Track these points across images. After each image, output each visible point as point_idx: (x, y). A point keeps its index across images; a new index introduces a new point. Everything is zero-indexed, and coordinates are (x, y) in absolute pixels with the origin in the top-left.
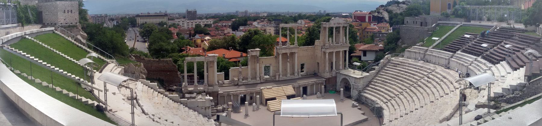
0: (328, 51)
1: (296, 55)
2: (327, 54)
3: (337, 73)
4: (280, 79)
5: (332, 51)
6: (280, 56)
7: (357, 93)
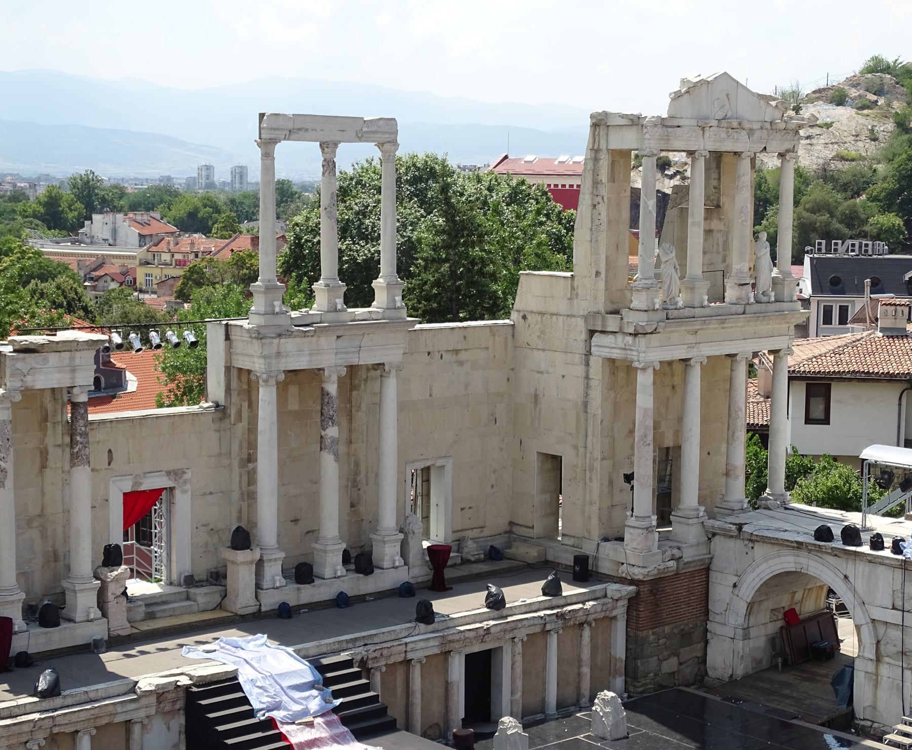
0: (651, 353)
1: (391, 386)
2: (645, 380)
6: (266, 397)
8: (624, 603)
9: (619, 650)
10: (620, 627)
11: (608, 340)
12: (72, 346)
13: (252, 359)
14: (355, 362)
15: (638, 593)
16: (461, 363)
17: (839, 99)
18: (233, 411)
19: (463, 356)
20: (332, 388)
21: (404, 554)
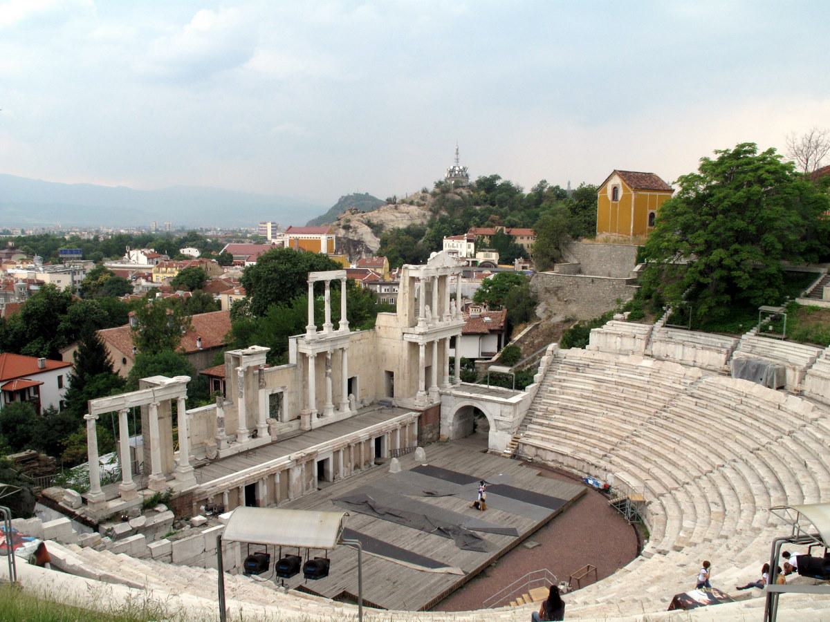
0: (422, 341)
1: (346, 355)
2: (422, 349)
3: (441, 394)
5: (432, 340)
6: (311, 363)
7: (508, 438)
8: (417, 419)
9: (416, 433)
10: (416, 425)
11: (409, 336)
12: (261, 352)
13: (310, 351)
15: (421, 415)
16: (361, 343)
17: (411, 203)
18: (299, 366)
19: (361, 341)
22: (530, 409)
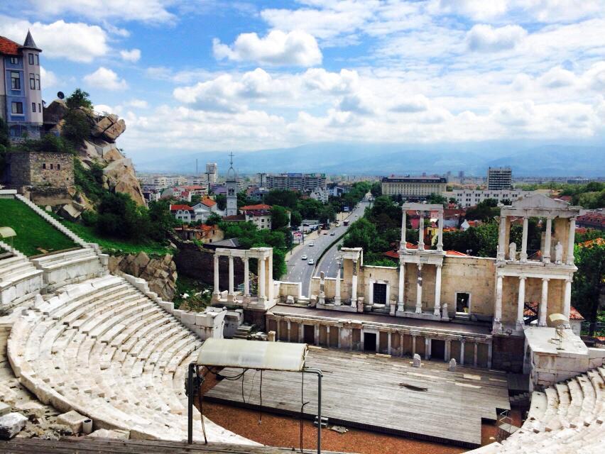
1: (439, 271)
4: (398, 314)
5: (514, 274)
9: (490, 354)
10: (490, 348)
14: (426, 262)
19: (476, 266)
20: (420, 268)
21: (441, 311)
22: (584, 373)
